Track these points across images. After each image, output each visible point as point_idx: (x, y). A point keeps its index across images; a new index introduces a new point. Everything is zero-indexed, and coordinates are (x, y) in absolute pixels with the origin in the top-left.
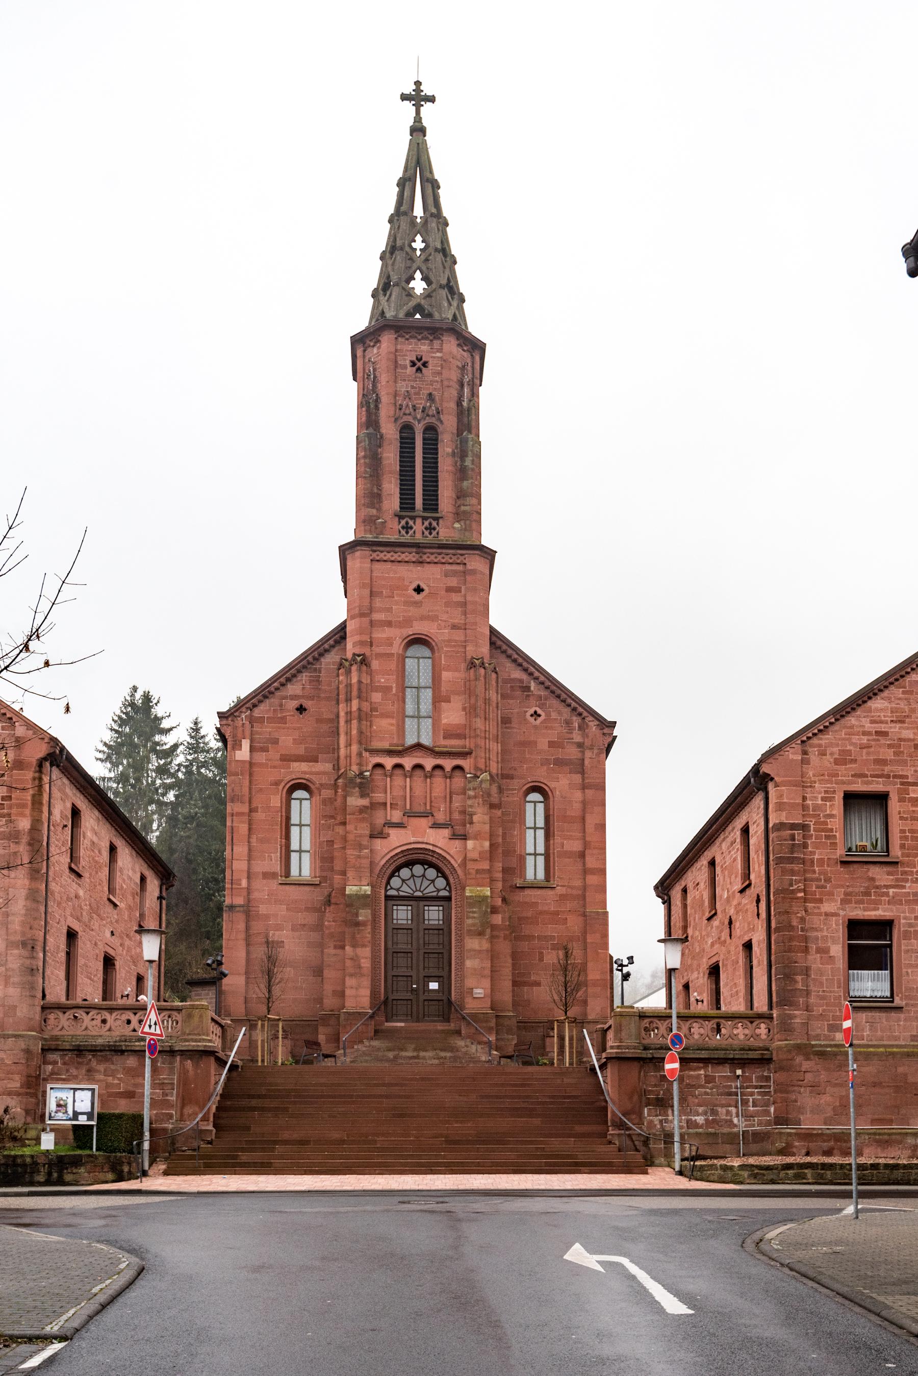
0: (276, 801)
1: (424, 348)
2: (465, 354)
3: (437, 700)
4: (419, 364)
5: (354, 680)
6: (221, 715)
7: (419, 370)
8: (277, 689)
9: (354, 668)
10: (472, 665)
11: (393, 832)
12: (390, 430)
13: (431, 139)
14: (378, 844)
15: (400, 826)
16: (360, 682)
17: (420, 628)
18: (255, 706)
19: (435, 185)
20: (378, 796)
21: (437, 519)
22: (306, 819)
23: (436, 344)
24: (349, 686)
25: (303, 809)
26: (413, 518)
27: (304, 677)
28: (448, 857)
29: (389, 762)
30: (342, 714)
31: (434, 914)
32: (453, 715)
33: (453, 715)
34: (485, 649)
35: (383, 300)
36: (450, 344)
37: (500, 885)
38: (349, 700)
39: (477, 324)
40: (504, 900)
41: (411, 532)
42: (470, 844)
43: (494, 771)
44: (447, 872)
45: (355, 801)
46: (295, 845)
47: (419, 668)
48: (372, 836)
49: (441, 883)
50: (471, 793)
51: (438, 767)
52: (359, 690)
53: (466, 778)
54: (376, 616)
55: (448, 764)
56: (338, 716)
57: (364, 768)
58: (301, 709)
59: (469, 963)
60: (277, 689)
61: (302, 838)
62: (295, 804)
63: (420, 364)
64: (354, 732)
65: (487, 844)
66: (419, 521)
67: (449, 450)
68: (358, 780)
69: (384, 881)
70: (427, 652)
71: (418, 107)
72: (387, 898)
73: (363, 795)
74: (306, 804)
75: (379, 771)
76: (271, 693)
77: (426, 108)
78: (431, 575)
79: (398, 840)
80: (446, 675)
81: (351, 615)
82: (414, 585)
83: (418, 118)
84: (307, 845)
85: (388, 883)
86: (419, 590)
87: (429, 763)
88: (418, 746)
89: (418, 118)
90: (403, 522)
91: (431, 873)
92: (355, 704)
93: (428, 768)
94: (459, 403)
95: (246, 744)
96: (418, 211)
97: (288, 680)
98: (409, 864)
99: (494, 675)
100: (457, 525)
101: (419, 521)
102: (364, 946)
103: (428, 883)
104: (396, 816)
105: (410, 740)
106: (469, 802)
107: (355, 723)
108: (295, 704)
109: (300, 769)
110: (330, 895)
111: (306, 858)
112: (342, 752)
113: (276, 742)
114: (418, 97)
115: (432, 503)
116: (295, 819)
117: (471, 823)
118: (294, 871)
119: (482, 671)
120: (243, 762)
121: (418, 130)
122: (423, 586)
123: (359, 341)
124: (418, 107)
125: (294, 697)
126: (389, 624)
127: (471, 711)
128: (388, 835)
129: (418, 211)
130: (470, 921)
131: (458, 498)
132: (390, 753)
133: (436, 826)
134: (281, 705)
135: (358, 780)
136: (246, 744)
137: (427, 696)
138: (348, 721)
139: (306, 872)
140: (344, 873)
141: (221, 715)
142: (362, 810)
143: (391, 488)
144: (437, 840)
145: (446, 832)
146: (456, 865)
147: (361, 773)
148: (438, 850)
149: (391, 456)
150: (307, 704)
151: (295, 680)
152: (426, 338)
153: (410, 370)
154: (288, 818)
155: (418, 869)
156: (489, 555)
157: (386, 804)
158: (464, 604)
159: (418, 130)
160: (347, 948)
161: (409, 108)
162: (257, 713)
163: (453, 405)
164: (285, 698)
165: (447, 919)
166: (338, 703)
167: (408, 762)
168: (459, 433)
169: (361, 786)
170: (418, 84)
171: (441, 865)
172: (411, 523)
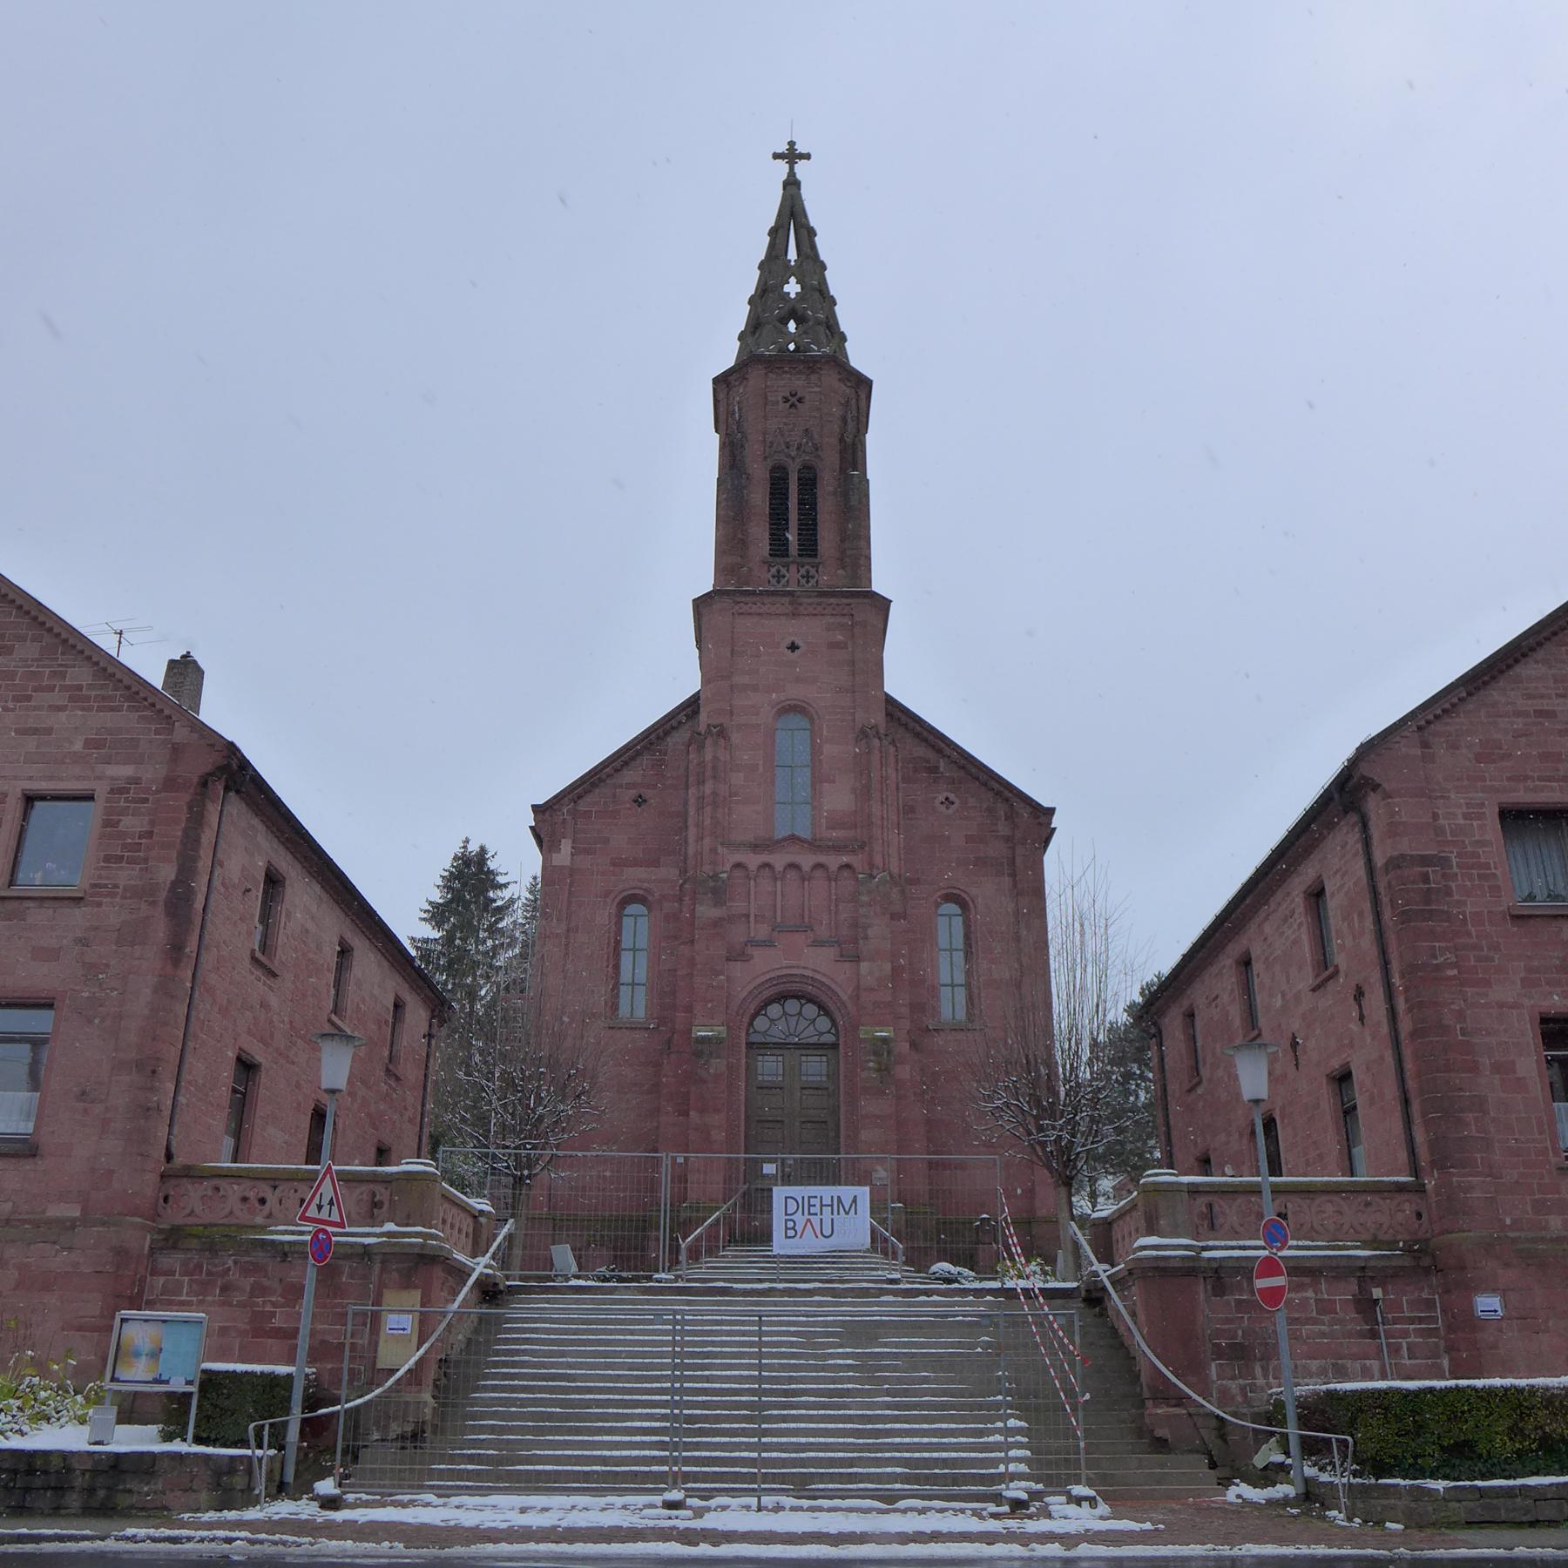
0: (603, 916)
1: (798, 383)
2: (848, 391)
3: (819, 779)
4: (793, 400)
5: (708, 757)
6: (535, 808)
7: (792, 405)
8: (609, 776)
9: (709, 742)
10: (864, 734)
11: (757, 953)
12: (759, 472)
13: (806, 192)
14: (737, 969)
15: (768, 944)
16: (715, 758)
17: (795, 692)
18: (580, 797)
19: (812, 233)
20: (738, 906)
21: (816, 566)
22: (643, 942)
23: (814, 377)
24: (702, 764)
25: (638, 928)
26: (787, 566)
27: (646, 760)
28: (833, 986)
29: (753, 861)
30: (692, 801)
31: (814, 1067)
32: (839, 798)
33: (839, 798)
34: (878, 718)
35: (750, 340)
36: (830, 378)
37: (906, 1024)
38: (701, 782)
39: (858, 358)
40: (914, 1045)
41: (784, 581)
42: (864, 966)
43: (895, 871)
44: (832, 1007)
45: (706, 911)
46: (626, 976)
47: (793, 742)
48: (728, 959)
49: (824, 1023)
50: (865, 898)
51: (819, 866)
52: (714, 768)
53: (857, 879)
54: (737, 679)
55: (833, 861)
56: (686, 804)
57: (720, 868)
58: (640, 801)
59: (864, 1135)
60: (609, 776)
61: (635, 967)
62: (627, 922)
63: (794, 400)
64: (708, 822)
65: (888, 967)
66: (793, 568)
67: (831, 489)
68: (712, 884)
69: (746, 1020)
70: (805, 723)
71: (792, 164)
72: (750, 1045)
73: (718, 903)
74: (644, 923)
75: (738, 873)
76: (600, 780)
77: (800, 167)
78: (810, 629)
79: (766, 964)
80: (829, 750)
81: (705, 681)
82: (788, 642)
83: (792, 173)
84: (642, 975)
85: (751, 1024)
86: (793, 647)
87: (807, 861)
88: (793, 838)
89: (792, 173)
90: (774, 570)
91: (811, 1010)
92: (708, 788)
93: (806, 867)
94: (842, 440)
95: (566, 846)
96: (792, 255)
97: (626, 764)
98: (781, 998)
99: (892, 749)
100: (840, 572)
101: (793, 568)
102: (717, 1111)
103: (810, 1025)
104: (762, 931)
105: (781, 833)
106: (862, 911)
107: (708, 809)
108: (633, 793)
109: (636, 876)
110: (669, 1041)
111: (641, 993)
112: (691, 851)
113: (606, 841)
114: (792, 155)
115: (809, 547)
116: (627, 942)
117: (866, 938)
118: (624, 1010)
119: (876, 742)
120: (563, 867)
121: (792, 184)
122: (798, 642)
123: (722, 383)
124: (792, 164)
125: (629, 786)
126: (755, 689)
127: (863, 794)
128: (752, 957)
129: (792, 255)
130: (864, 1074)
131: (842, 541)
132: (755, 847)
133: (818, 943)
134: (614, 795)
135: (712, 884)
136: (566, 846)
137: (804, 777)
138: (700, 809)
139: (641, 1013)
140: (689, 1009)
141: (535, 808)
142: (716, 923)
143: (760, 534)
144: (818, 963)
145: (831, 952)
146: (845, 998)
147: (715, 877)
148: (818, 977)
149: (759, 498)
150: (647, 793)
151: (633, 764)
152: (800, 372)
153: (782, 406)
154: (618, 942)
155: (792, 1006)
156: (883, 605)
157: (748, 916)
158: (853, 663)
159: (792, 184)
160: (692, 1113)
161: (782, 167)
162: (582, 806)
163: (835, 441)
164: (621, 786)
165: (833, 1075)
166: (687, 788)
167: (779, 860)
168: (843, 470)
169: (715, 891)
170: (792, 144)
171: (824, 998)
172: (783, 571)
